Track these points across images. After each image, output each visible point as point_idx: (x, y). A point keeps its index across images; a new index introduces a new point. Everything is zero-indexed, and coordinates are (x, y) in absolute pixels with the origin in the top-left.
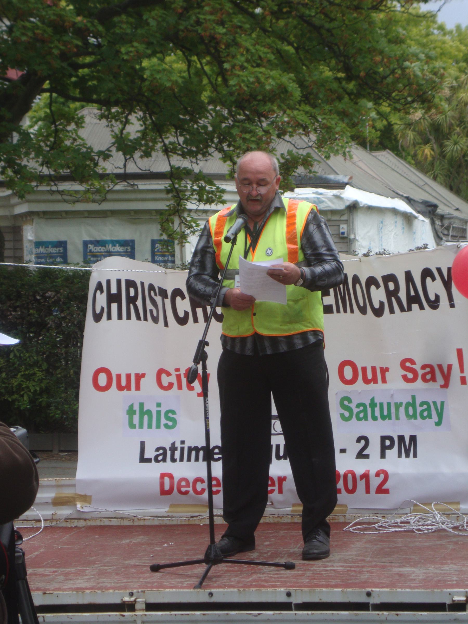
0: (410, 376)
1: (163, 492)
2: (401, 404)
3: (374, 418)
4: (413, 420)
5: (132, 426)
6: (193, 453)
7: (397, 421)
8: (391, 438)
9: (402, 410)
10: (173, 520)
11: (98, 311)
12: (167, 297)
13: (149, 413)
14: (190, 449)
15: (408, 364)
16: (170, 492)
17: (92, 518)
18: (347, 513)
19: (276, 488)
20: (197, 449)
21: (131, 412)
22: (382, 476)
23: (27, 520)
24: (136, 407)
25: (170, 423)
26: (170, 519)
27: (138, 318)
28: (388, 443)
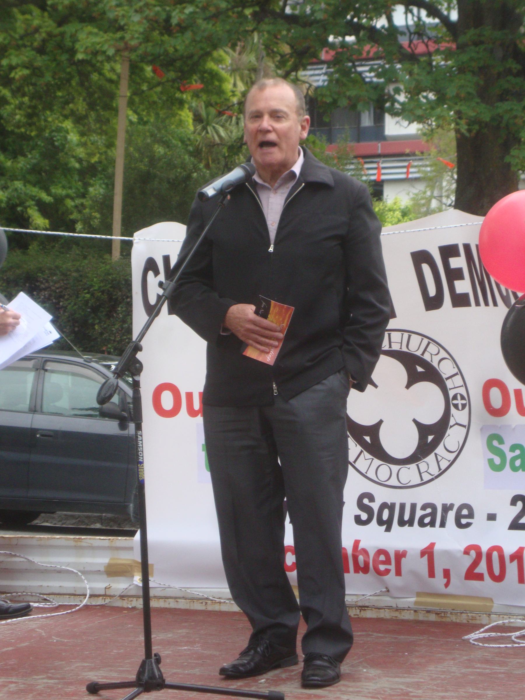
11: (153, 300)
18: (493, 610)
19: (392, 567)
23: (75, 595)
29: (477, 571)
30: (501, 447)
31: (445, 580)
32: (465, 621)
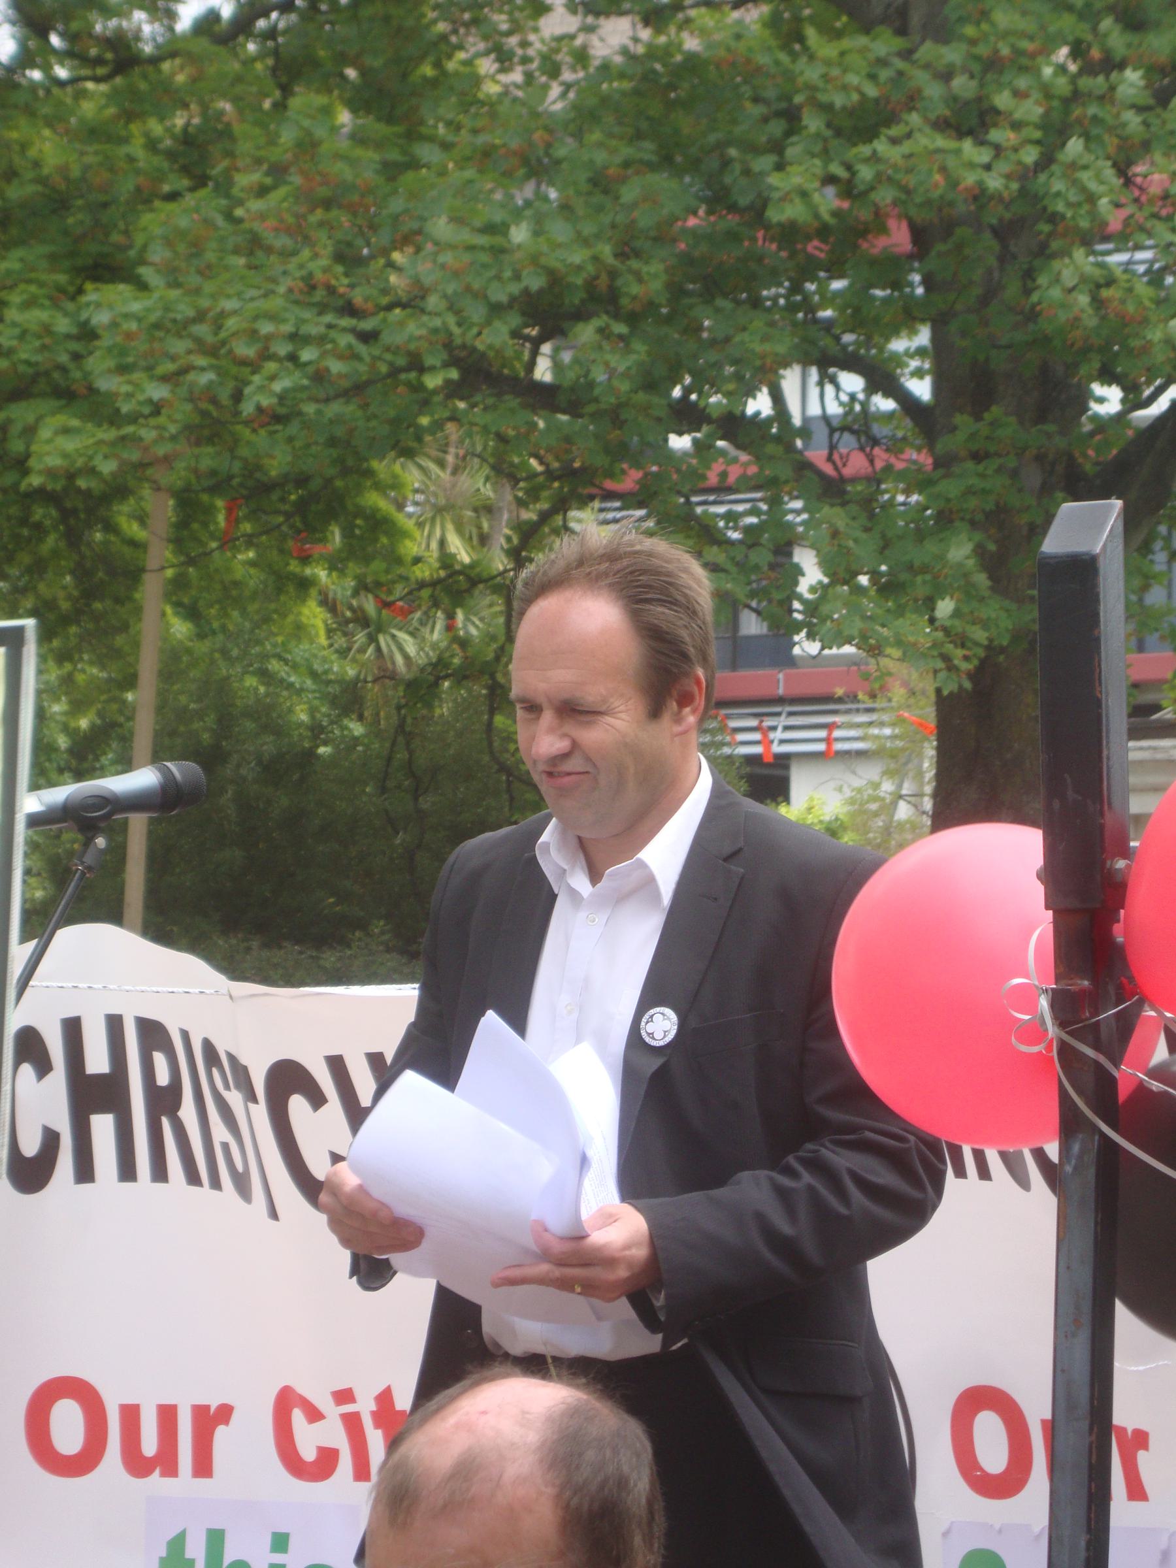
11: (30, 1147)
27: (193, 1178)
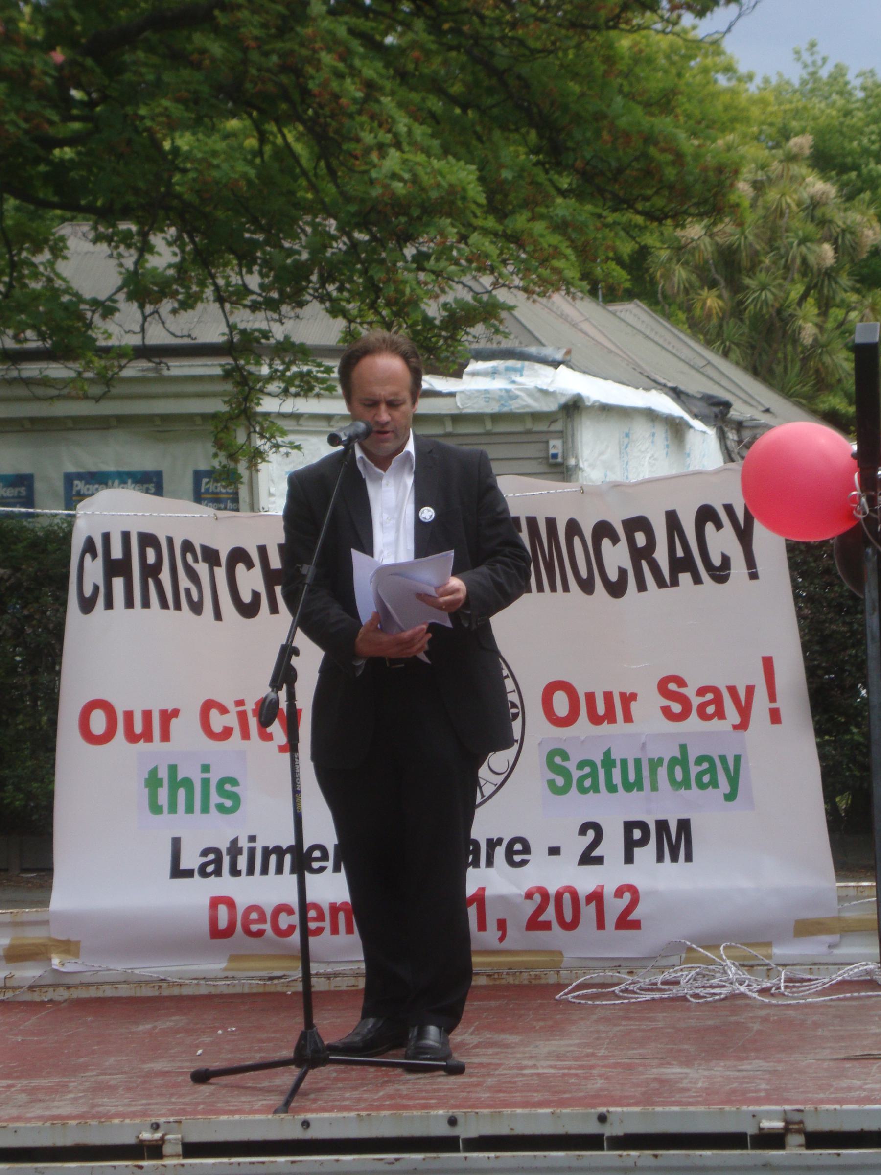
0: (677, 708)
1: (216, 933)
2: (660, 761)
3: (612, 788)
4: (683, 791)
5: (156, 808)
6: (273, 859)
7: (654, 793)
8: (642, 826)
9: (662, 772)
10: (234, 985)
11: (88, 592)
12: (219, 565)
13: (187, 783)
14: (267, 852)
15: (672, 687)
16: (229, 932)
17: (82, 984)
20: (279, 852)
21: (153, 781)
22: (627, 896)
24: (163, 774)
25: (228, 803)
26: (228, 982)
27: (164, 605)
28: (637, 834)
29: (542, 918)
30: (565, 764)
31: (500, 933)
32: (526, 982)
